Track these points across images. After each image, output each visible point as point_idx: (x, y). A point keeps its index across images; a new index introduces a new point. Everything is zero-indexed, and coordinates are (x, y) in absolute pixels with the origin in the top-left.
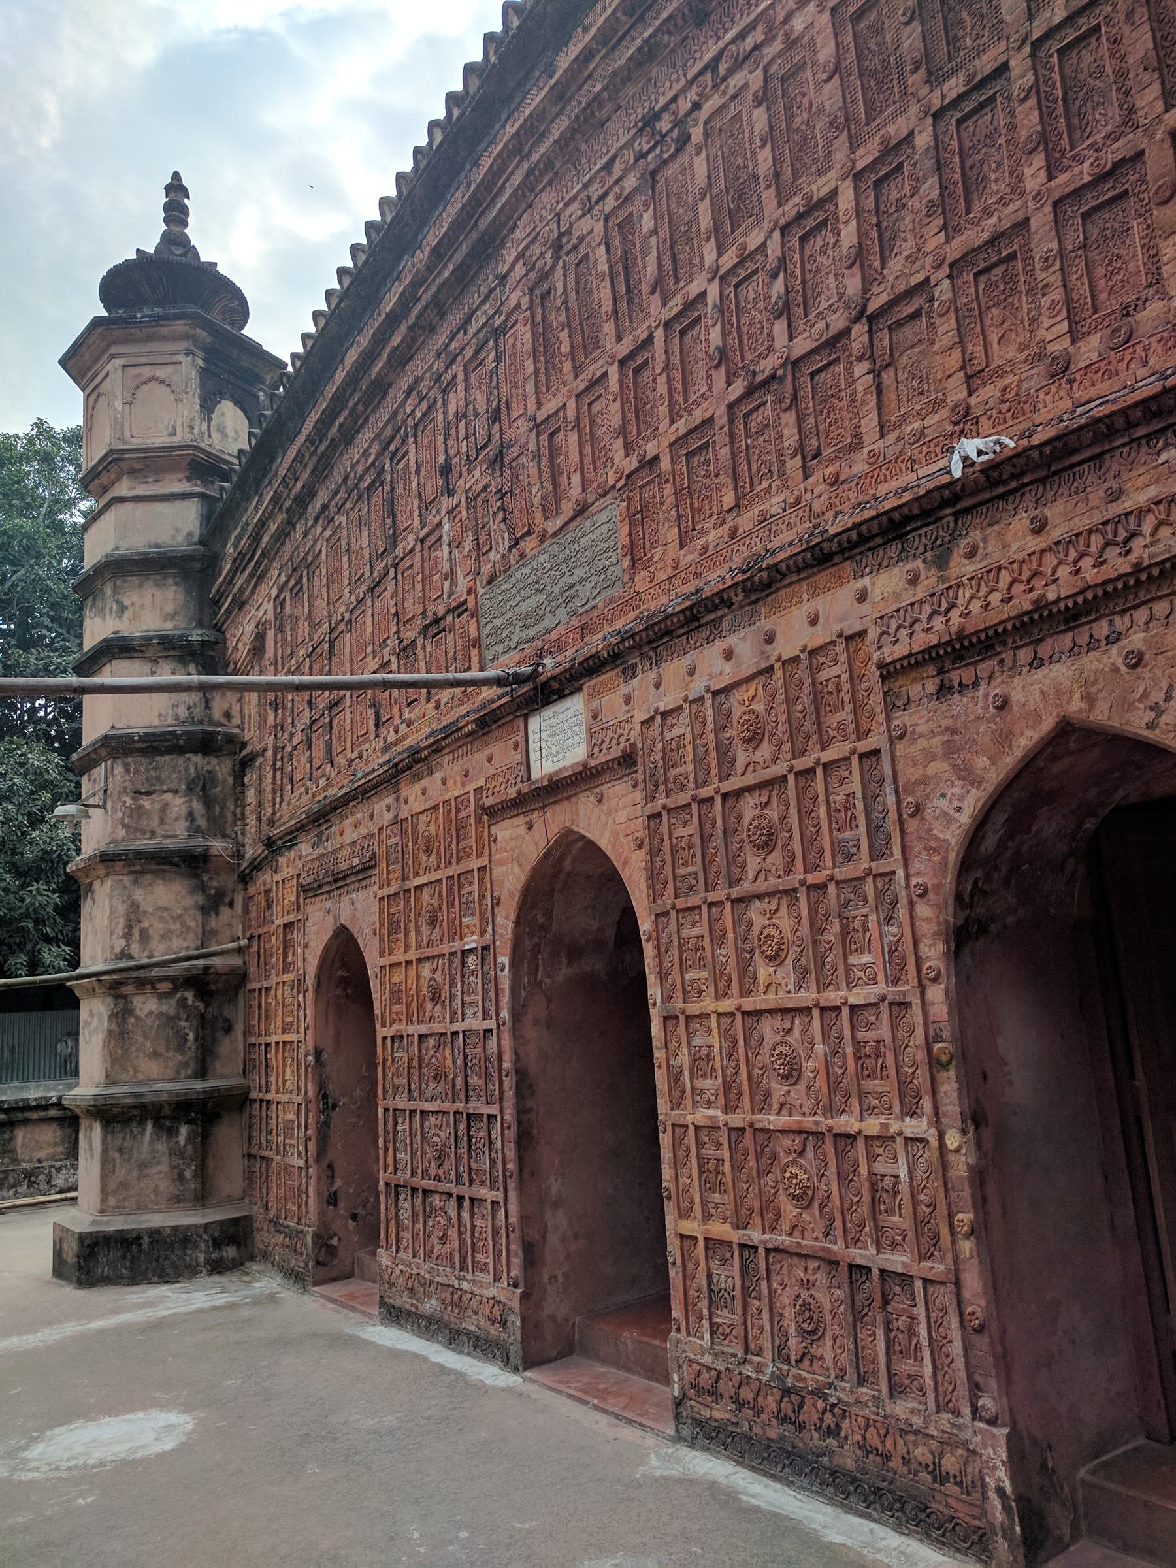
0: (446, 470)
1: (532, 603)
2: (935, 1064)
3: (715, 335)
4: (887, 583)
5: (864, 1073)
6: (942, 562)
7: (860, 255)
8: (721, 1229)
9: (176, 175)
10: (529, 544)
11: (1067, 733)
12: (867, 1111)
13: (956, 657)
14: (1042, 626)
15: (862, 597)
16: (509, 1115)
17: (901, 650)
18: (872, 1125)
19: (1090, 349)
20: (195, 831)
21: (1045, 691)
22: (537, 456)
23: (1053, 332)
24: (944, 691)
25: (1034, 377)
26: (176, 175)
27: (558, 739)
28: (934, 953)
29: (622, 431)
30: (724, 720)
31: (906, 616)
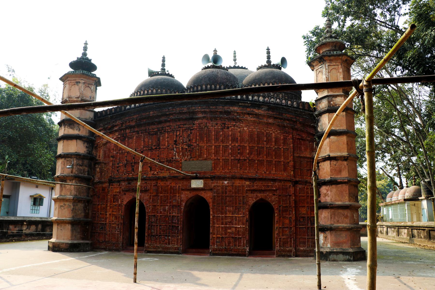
0: (176, 141)
1: (194, 166)
2: (247, 221)
3: (230, 151)
4: (247, 183)
5: (239, 222)
6: (254, 183)
7: (248, 154)
8: (218, 236)
9: (86, 41)
10: (194, 159)
11: (262, 199)
12: (239, 225)
13: (253, 191)
14: (261, 191)
15: (245, 183)
16: (182, 226)
17: (249, 189)
18: (239, 226)
19: (268, 173)
20: (88, 174)
21: (260, 195)
22: (198, 149)
23: (265, 169)
24: (251, 193)
25: (263, 173)
26: (86, 41)
27: (196, 184)
28: (247, 213)
29: (214, 153)
30: (226, 189)
31: (249, 186)
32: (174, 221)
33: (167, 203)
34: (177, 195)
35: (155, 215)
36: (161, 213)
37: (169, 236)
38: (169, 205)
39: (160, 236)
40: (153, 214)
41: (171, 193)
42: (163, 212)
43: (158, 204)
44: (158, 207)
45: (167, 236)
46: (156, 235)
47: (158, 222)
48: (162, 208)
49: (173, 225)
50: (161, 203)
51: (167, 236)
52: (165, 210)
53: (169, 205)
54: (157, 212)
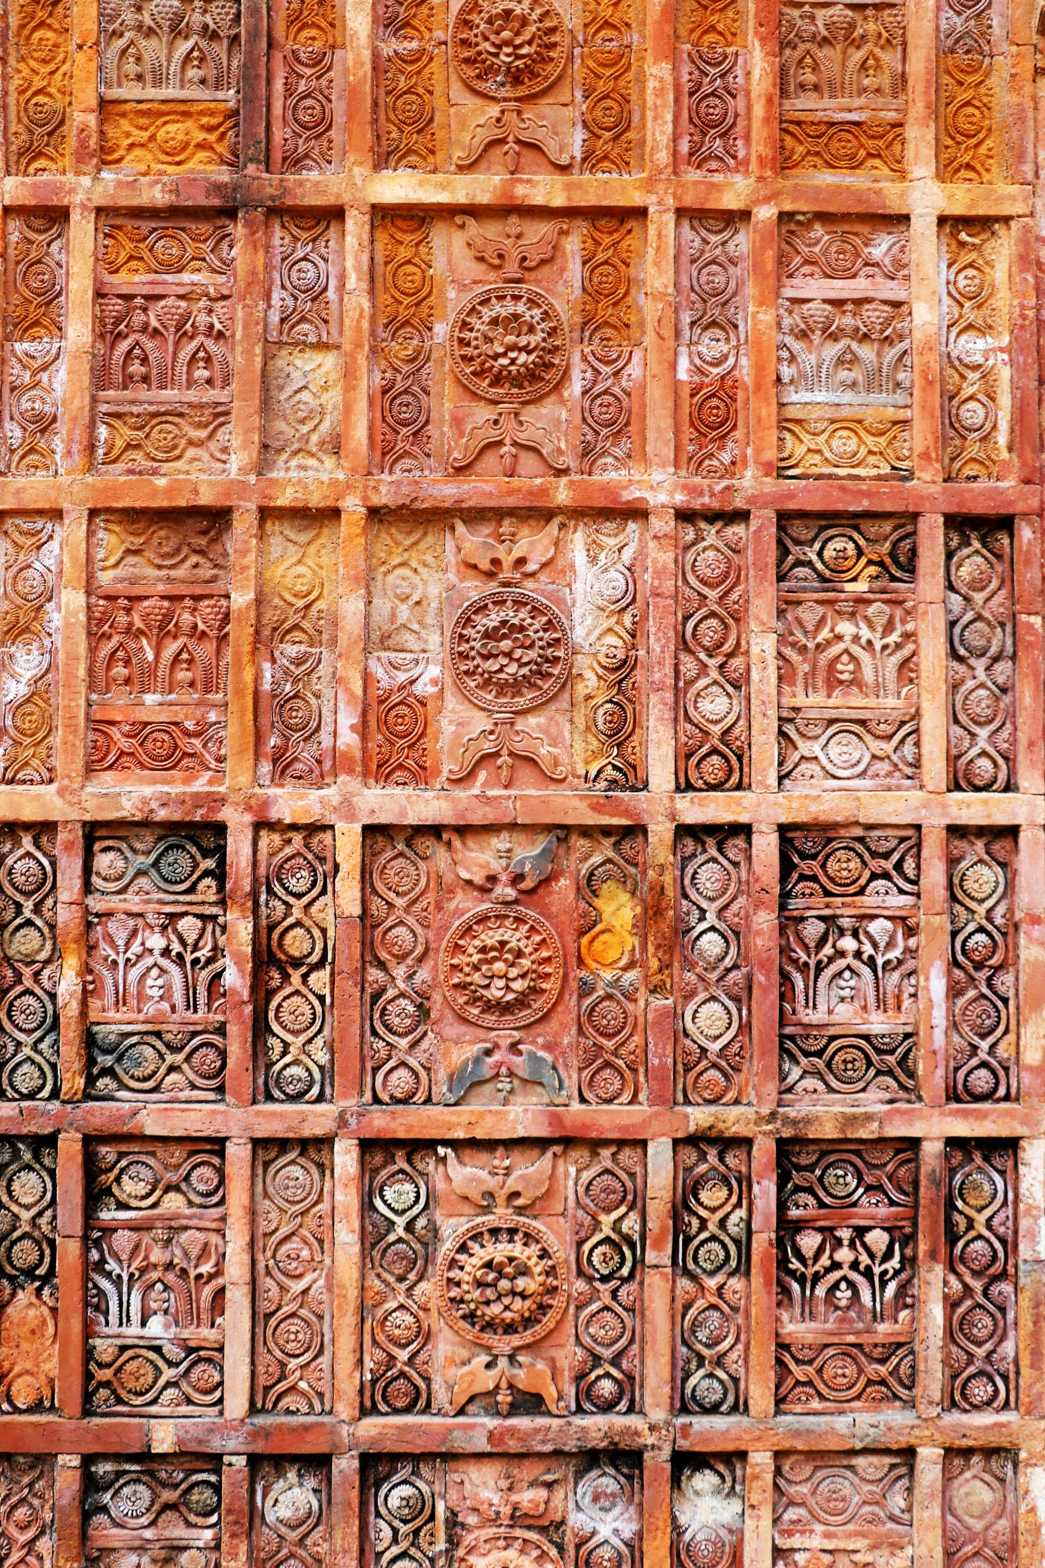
32: (837, 1006)
33: (612, 424)
34: (926, 196)
35: (202, 835)
36: (395, 739)
37: (687, 1462)
38: (659, 486)
39: (376, 1466)
40: (132, 794)
41: (708, 126)
42: (459, 724)
43: (303, 479)
44: (296, 565)
45: (624, 1458)
46: (265, 1464)
47: (300, 1056)
48: (433, 579)
49: (822, 1109)
50: (400, 425)
51: (624, 1458)
52: (514, 652)
53: (659, 486)
54: (281, 733)
